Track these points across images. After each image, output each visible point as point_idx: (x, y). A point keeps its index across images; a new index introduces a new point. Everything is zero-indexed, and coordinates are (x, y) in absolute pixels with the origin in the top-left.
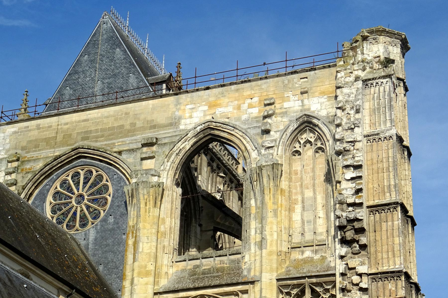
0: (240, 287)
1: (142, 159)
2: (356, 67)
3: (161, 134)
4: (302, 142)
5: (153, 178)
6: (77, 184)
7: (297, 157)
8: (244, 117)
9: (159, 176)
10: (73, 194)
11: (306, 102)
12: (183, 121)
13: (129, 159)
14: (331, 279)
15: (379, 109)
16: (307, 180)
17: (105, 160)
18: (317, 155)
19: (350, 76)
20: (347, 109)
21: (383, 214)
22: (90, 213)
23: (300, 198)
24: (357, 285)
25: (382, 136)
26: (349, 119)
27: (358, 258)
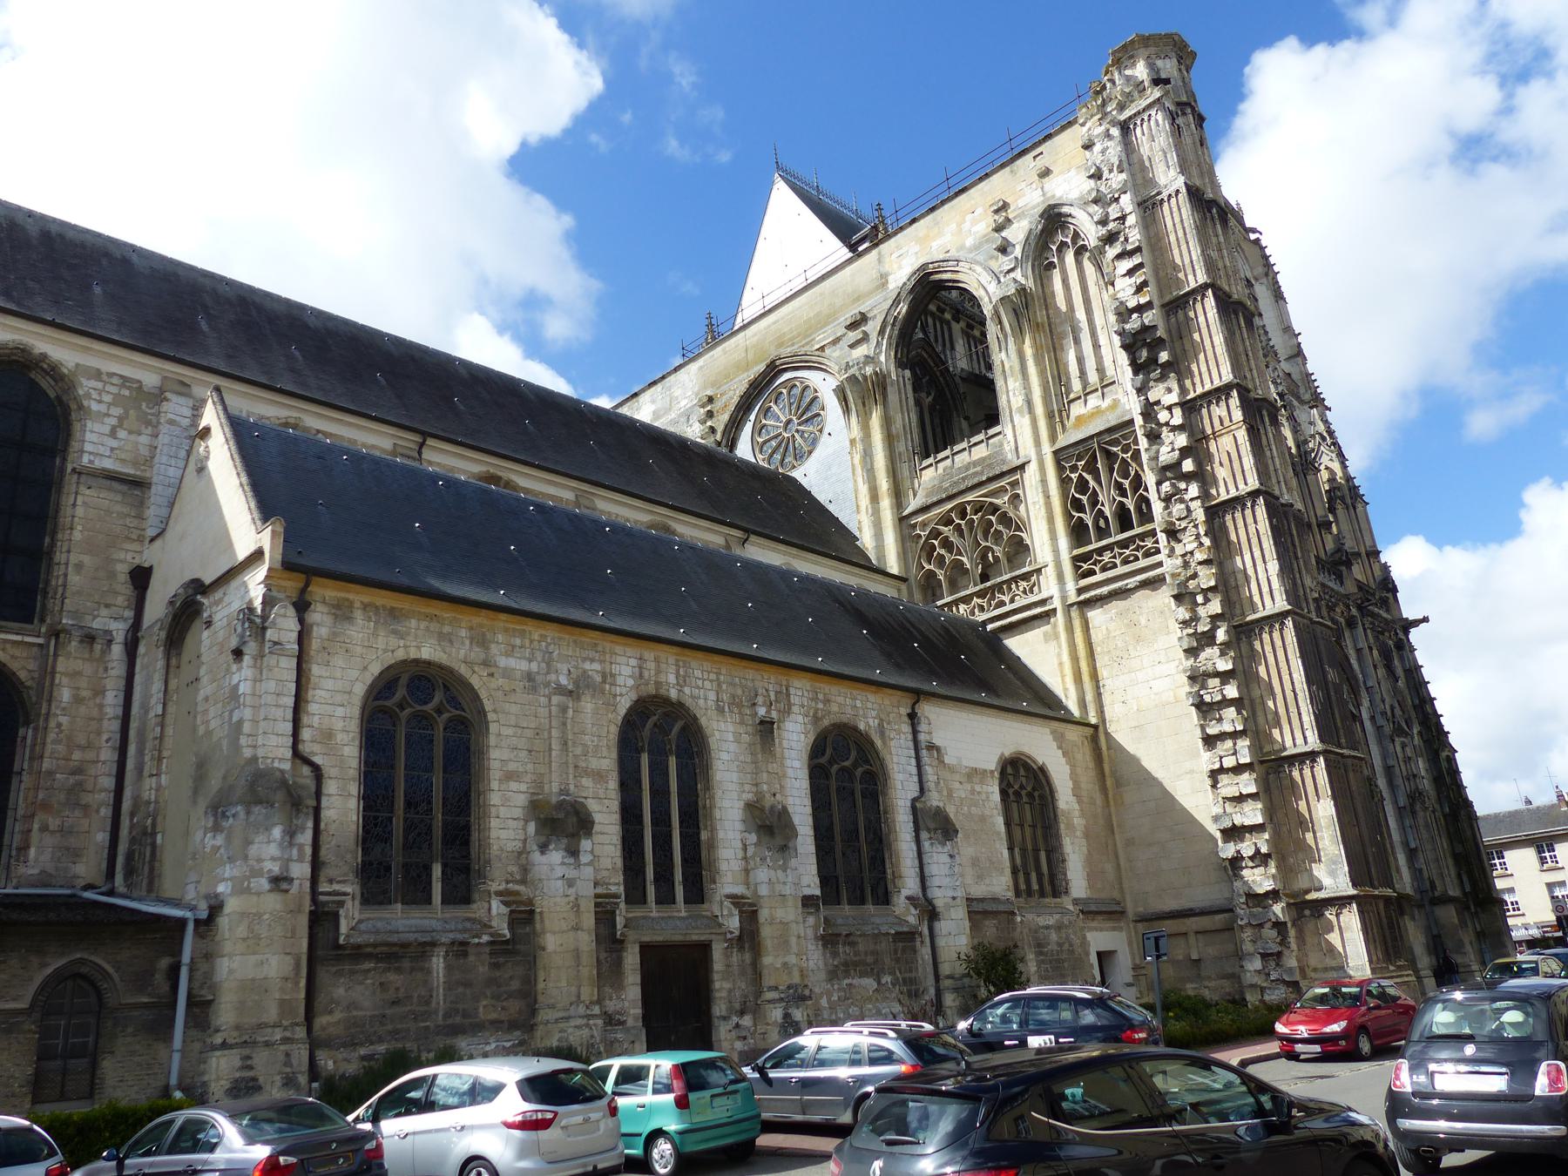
8: (969, 242)
24: (1167, 424)
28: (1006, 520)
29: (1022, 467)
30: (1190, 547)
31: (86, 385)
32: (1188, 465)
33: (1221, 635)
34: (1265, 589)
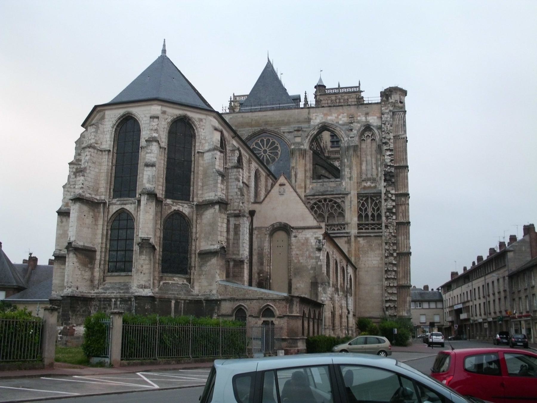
1: (295, 137)
2: (389, 105)
3: (303, 125)
8: (341, 122)
9: (303, 145)
11: (367, 118)
12: (312, 121)
16: (368, 153)
17: (277, 135)
23: (365, 159)
25: (401, 137)
28: (339, 206)
29: (347, 194)
31: (244, 158)
32: (394, 210)
33: (395, 254)
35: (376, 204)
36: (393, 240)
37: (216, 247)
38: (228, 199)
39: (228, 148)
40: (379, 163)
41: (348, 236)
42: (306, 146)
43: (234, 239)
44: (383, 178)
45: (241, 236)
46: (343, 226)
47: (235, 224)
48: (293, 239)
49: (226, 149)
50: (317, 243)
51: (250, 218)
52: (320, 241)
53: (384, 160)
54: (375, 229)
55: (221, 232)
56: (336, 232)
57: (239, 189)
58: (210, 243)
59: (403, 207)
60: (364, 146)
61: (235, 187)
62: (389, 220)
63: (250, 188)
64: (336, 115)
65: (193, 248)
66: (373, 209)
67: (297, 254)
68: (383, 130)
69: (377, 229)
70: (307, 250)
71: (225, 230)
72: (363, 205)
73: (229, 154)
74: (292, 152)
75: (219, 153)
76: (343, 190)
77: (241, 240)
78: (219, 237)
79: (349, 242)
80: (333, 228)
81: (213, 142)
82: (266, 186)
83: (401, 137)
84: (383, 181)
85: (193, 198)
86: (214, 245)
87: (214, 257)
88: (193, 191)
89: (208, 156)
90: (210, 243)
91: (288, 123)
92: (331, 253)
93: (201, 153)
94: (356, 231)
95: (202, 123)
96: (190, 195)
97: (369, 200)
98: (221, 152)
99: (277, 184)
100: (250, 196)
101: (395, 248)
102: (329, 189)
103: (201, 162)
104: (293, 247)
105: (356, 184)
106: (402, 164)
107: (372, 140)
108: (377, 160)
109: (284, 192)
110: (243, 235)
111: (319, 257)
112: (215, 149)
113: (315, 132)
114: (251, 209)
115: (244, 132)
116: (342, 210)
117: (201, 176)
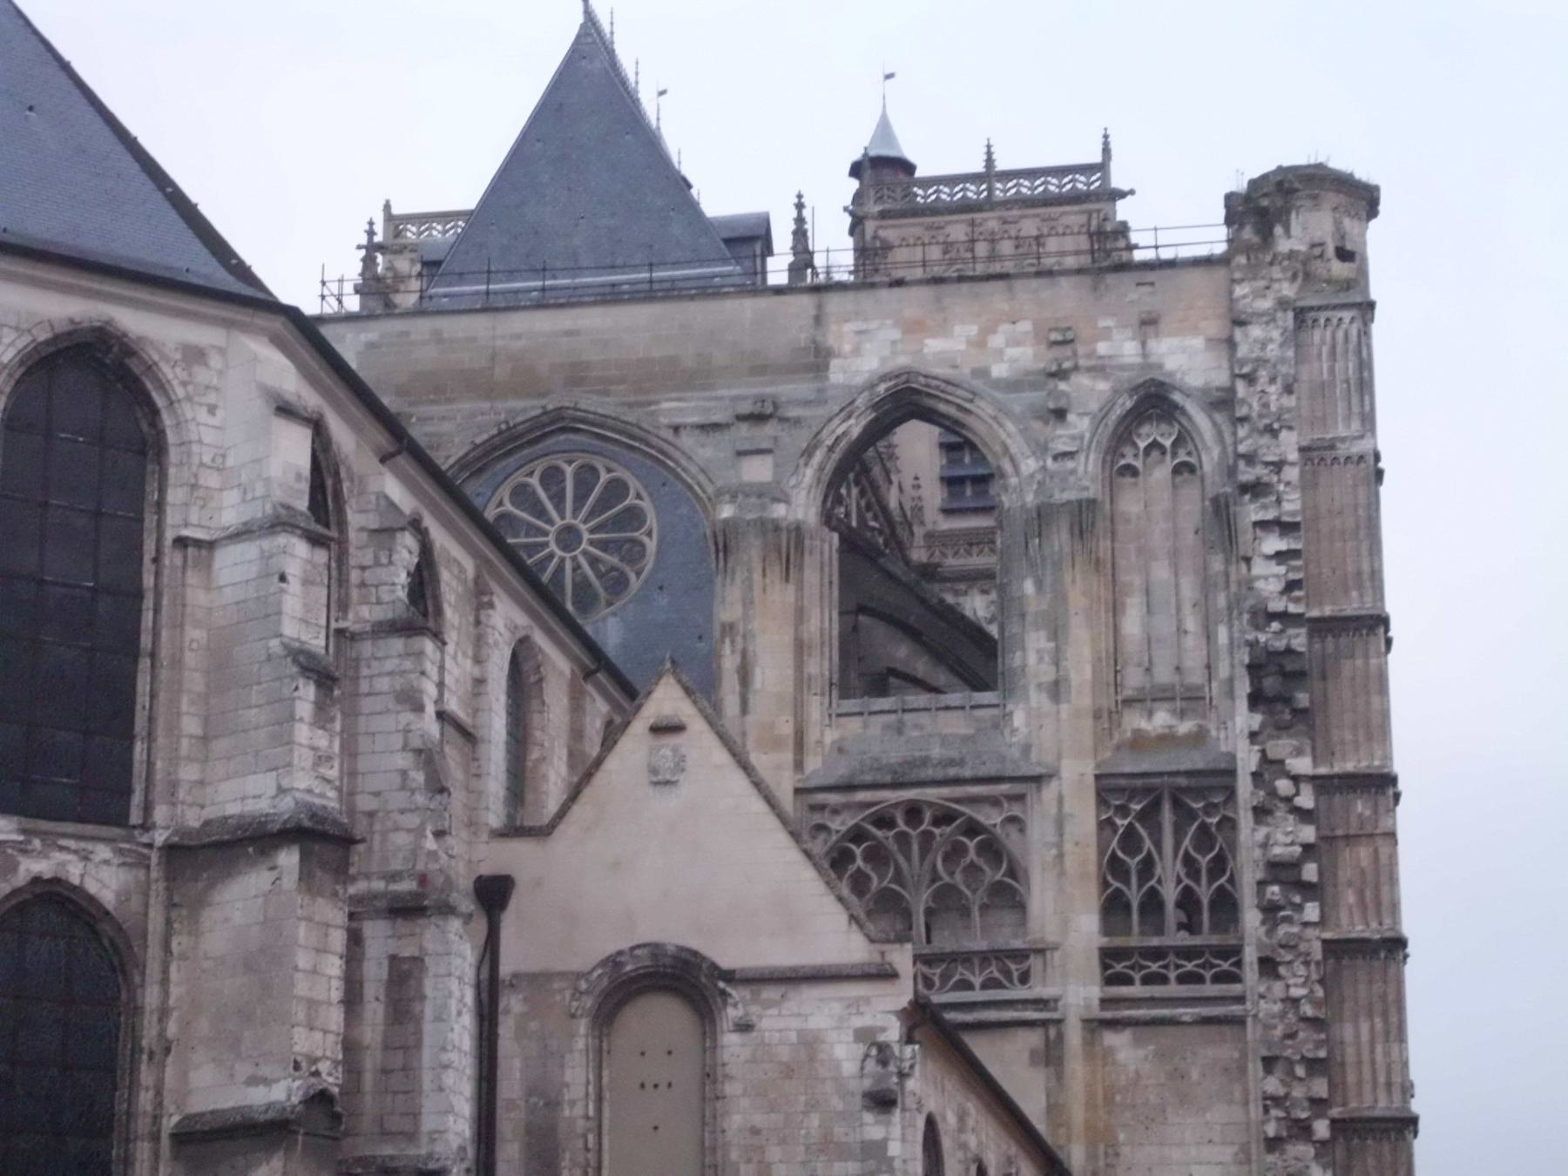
0: (1004, 788)
1: (741, 454)
2: (1276, 272)
4: (1142, 445)
5: (775, 506)
6: (558, 499)
7: (1128, 480)
8: (999, 371)
9: (787, 501)
10: (550, 522)
11: (1152, 344)
12: (835, 363)
13: (703, 452)
14: (1224, 781)
15: (1333, 384)
18: (1179, 479)
19: (1264, 296)
20: (1262, 380)
21: (1343, 640)
22: (600, 576)
23: (1137, 580)
24: (1288, 800)
25: (1342, 450)
26: (1266, 405)
27: (1290, 736)
28: (993, 850)
30: (1296, 992)
31: (445, 575)
33: (1322, 1129)
34: (1382, 1079)
35: (1204, 838)
36: (1308, 1043)
37: (282, 1092)
38: (352, 812)
39: (354, 519)
40: (1222, 601)
41: (1044, 1023)
42: (802, 506)
43: (387, 1047)
44: (1243, 687)
45: (428, 1027)
46: (1016, 961)
47: (393, 959)
48: (731, 1042)
49: (342, 525)
50: (871, 1066)
51: (480, 925)
52: (883, 1054)
53: (1248, 584)
54: (1199, 979)
55: (312, 1004)
56: (977, 995)
57: (419, 752)
58: (243, 1070)
59: (1364, 853)
60: (1130, 503)
61: (397, 741)
62: (1283, 930)
63: (482, 748)
64: (973, 330)
65: (145, 1100)
66: (1189, 861)
67: (755, 1131)
68: (1241, 411)
69: (1217, 979)
70: (812, 1106)
71: (336, 995)
72: (1130, 840)
73: (360, 553)
74: (724, 543)
75: (301, 548)
76: (1016, 753)
77: (427, 1056)
78: (300, 1034)
79: (1051, 1057)
80: (961, 972)
81: (268, 481)
82: (577, 734)
83: (1342, 450)
84: (1242, 704)
85: (148, 808)
86: (266, 1082)
87: (271, 1149)
88: (150, 764)
89: (235, 566)
90: (243, 1070)
91: (694, 378)
92: (948, 1123)
93: (198, 543)
94: (1095, 991)
95: (202, 375)
96: (128, 792)
97: (1167, 816)
98: (315, 541)
99: (639, 726)
100: (480, 793)
101: (1320, 1088)
102: (936, 752)
103: (197, 597)
104: (730, 1089)
105: (1087, 723)
106: (1352, 606)
107: (1177, 470)
108: (1207, 586)
109: (680, 765)
110: (438, 1019)
111: (882, 1145)
112: (279, 523)
113: (855, 427)
114: (486, 870)
115: (447, 427)
116: (1012, 873)
117: (195, 681)
